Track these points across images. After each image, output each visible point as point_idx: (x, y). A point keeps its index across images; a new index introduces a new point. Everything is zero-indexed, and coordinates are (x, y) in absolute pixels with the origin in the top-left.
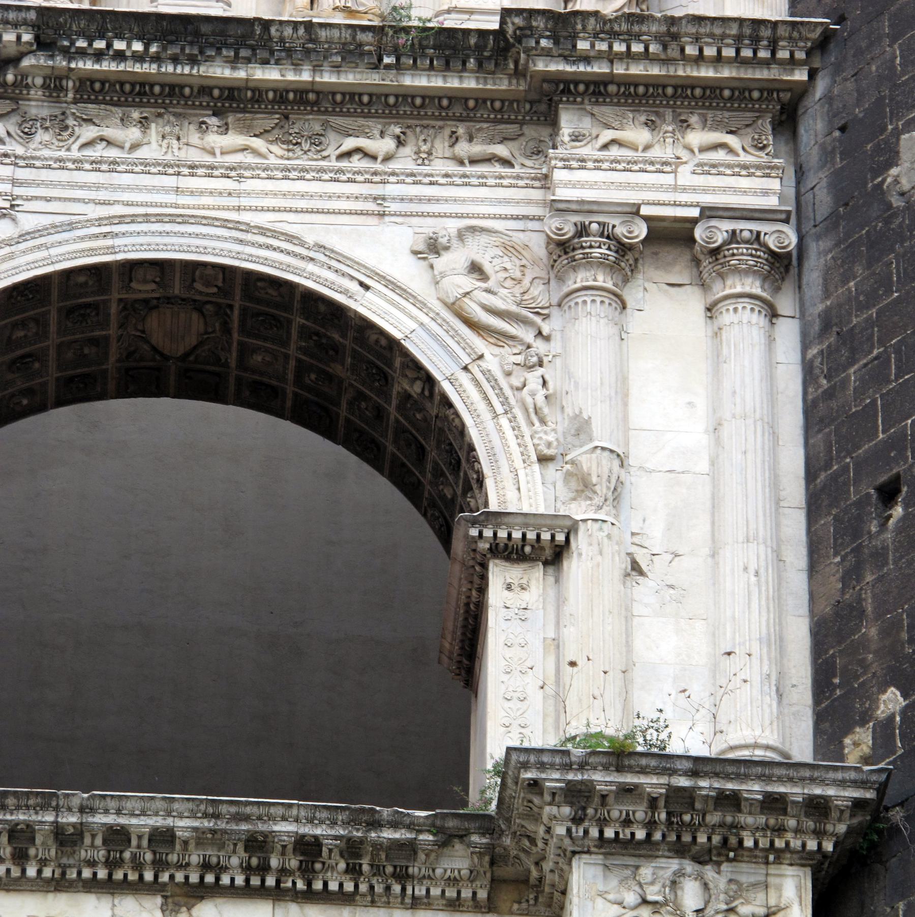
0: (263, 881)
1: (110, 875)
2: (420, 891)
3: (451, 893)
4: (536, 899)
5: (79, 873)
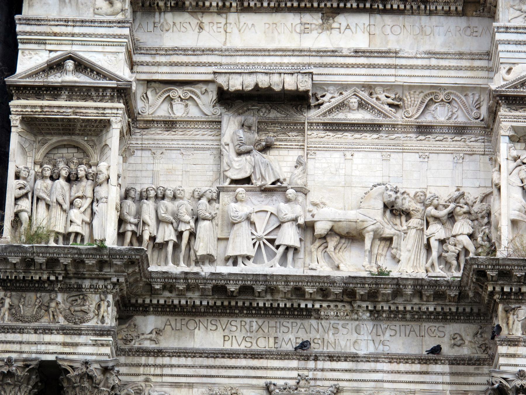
0: (365, 5)
1: (299, 5)
2: (433, 8)
3: (446, 8)
4: (483, 9)
5: (286, 4)
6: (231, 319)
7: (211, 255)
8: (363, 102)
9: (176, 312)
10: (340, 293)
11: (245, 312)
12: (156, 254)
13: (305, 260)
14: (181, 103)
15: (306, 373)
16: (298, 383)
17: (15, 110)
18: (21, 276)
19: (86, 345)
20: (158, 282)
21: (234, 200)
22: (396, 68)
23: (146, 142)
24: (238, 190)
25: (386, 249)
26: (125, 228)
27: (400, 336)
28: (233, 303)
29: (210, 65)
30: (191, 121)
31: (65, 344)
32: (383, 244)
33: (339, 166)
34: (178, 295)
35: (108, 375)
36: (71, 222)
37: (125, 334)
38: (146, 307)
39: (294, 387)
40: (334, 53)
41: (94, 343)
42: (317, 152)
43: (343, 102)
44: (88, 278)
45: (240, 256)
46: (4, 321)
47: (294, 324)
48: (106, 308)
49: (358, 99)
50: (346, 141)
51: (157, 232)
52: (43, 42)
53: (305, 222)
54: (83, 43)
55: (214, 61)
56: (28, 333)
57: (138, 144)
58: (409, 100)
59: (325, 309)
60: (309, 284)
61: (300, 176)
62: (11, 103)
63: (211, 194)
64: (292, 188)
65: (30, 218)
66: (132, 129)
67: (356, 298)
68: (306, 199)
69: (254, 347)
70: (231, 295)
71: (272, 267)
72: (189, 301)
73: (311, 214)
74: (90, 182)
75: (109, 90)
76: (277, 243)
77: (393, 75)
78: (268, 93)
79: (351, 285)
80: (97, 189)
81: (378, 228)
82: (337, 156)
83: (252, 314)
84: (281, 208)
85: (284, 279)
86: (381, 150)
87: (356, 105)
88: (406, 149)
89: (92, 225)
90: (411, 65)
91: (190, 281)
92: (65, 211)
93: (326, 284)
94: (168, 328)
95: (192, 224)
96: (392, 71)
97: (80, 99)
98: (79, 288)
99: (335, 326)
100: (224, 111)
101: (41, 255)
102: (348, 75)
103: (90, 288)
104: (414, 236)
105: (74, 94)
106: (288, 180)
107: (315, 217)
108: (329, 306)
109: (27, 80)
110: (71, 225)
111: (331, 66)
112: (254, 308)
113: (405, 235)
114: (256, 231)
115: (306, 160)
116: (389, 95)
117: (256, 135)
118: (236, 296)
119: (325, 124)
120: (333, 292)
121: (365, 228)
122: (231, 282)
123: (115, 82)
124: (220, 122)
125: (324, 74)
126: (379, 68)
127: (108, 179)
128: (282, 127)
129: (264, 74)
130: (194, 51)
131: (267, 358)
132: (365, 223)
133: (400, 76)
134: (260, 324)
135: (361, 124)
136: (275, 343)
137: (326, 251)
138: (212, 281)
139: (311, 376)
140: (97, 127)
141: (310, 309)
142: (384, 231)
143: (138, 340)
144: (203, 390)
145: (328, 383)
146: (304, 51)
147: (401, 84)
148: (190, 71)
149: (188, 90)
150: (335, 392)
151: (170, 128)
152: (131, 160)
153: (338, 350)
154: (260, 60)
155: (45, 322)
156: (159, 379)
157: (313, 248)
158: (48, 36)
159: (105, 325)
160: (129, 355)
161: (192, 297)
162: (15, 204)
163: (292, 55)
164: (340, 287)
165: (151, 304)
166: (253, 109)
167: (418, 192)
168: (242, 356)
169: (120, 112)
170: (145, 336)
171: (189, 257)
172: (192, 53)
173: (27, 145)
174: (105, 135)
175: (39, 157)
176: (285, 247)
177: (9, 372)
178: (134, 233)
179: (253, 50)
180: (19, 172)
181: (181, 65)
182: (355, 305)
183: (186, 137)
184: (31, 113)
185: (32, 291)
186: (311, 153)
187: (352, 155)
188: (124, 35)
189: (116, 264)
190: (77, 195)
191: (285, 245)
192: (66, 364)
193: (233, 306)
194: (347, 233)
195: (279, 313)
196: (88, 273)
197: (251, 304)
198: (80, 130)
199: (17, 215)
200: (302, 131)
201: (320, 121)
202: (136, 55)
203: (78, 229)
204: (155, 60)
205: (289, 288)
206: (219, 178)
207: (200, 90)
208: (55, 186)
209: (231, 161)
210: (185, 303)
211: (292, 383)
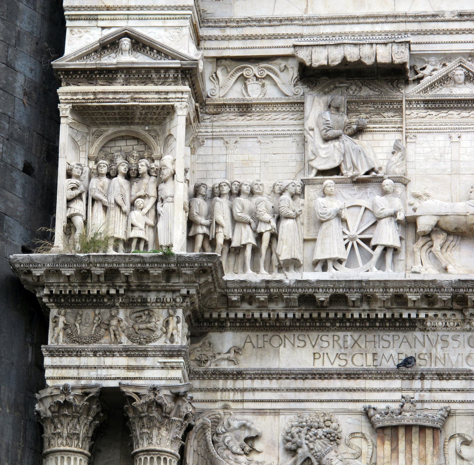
6: (321, 334)
7: (296, 259)
8: (471, 74)
9: (257, 326)
10: (449, 299)
11: (338, 325)
12: (232, 260)
13: (406, 262)
14: (257, 82)
15: (411, 394)
16: (402, 406)
17: (64, 97)
18: (77, 290)
19: (153, 368)
20: (234, 293)
21: (322, 194)
23: (217, 130)
26: (195, 230)
27: (333, 347)
28: (323, 315)
29: (289, 37)
30: (269, 104)
31: (129, 368)
33: (444, 151)
34: (259, 307)
35: (180, 403)
36: (132, 226)
37: (198, 354)
38: (222, 323)
39: (397, 412)
40: (434, 17)
41: (162, 365)
42: (418, 135)
43: (447, 75)
44: (154, 291)
45: (330, 259)
46: (58, 342)
47: (396, 338)
48: (175, 325)
49: (465, 70)
50: (452, 120)
51: (233, 234)
52: (95, 18)
53: (405, 217)
54: (141, 18)
55: (294, 32)
56: (87, 356)
57: (207, 132)
59: (432, 319)
60: (411, 290)
61: (398, 164)
62: (59, 90)
63: (294, 188)
64: (389, 178)
65: (85, 223)
66: (200, 115)
67: (468, 305)
68: (406, 190)
69: (350, 366)
70: (321, 306)
71: (368, 271)
72: (271, 313)
73: (412, 207)
74: (153, 179)
75: (172, 71)
76: (373, 243)
79: (461, 290)
80: (162, 186)
82: (441, 139)
83: (346, 327)
84: (377, 201)
85: (383, 285)
87: (462, 78)
89: (157, 229)
91: (272, 290)
92: (124, 213)
93: (432, 290)
94: (248, 345)
95: (273, 223)
97: (138, 83)
98: (144, 302)
99: (444, 338)
100: (307, 90)
101: (98, 265)
102: (452, 43)
103: (157, 302)
105: (132, 76)
106: (384, 168)
107: (417, 211)
108: (436, 316)
109: (78, 62)
110: (132, 229)
111: (432, 32)
112: (348, 320)
114: (348, 229)
115: (404, 145)
117: (346, 117)
118: (326, 307)
119: (426, 102)
120: (441, 299)
122: (321, 290)
123: (179, 61)
124: (303, 103)
125: (424, 43)
127: (173, 175)
129: (352, 46)
130: (271, 22)
131: (365, 378)
134: (356, 338)
135: (469, 100)
136: (374, 360)
137: (431, 251)
138: (298, 289)
139: (417, 398)
140: (159, 114)
141: (414, 319)
143: (213, 360)
144: (292, 417)
145: (437, 406)
146: (399, 16)
148: (267, 45)
149: (264, 68)
150: (446, 415)
151: (245, 112)
152: (201, 151)
153: (448, 366)
154: (347, 29)
155: (105, 342)
156: (239, 406)
157: (416, 247)
158: (100, 10)
159: (174, 344)
160: (204, 379)
161: (275, 308)
162: (68, 207)
163: (386, 22)
164: (448, 292)
165: (228, 319)
166: (340, 87)
168: (335, 376)
169: (186, 96)
170: (222, 356)
171: (271, 262)
172: (268, 24)
173: (79, 138)
174: (168, 123)
175: (93, 151)
176: (383, 247)
177: (65, 401)
178: (206, 236)
179: (339, 18)
180: (71, 170)
181: (256, 39)
182: (467, 314)
183: (264, 122)
184: (83, 101)
185: (90, 307)
186: (411, 136)
187: (459, 137)
188: (188, 6)
189: (185, 274)
190: (138, 194)
191: (382, 245)
192: (131, 390)
193: (323, 319)
194: (456, 229)
195: (378, 324)
196: (154, 284)
197: (344, 315)
198: (139, 119)
199: (70, 220)
200: (399, 111)
201: (420, 98)
202: (203, 29)
203: (141, 234)
204: (226, 34)
205: (389, 295)
206: (304, 169)
207: (278, 66)
208: (112, 184)
210: (267, 316)
211: (395, 406)
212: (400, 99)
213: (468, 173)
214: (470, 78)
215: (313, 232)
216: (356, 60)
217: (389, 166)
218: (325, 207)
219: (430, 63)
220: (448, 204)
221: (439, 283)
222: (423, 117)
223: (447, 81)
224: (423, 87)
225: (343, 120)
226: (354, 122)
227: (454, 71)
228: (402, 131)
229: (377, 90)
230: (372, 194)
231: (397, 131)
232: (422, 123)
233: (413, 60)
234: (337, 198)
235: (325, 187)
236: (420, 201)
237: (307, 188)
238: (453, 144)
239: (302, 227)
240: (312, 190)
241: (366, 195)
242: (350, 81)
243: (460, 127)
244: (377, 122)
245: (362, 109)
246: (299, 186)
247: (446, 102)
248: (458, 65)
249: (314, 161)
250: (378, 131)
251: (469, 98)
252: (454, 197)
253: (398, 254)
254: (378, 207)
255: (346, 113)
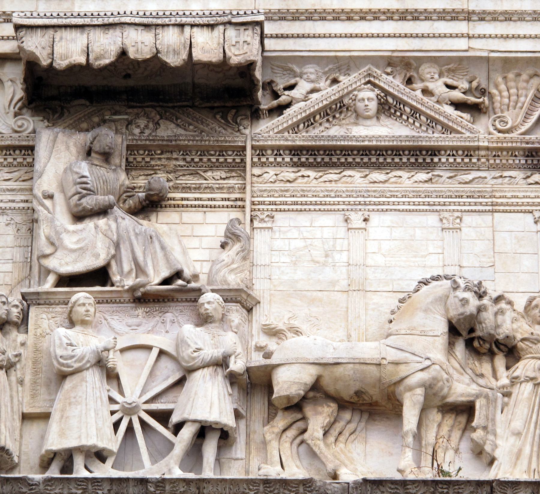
8: (390, 100)
22: (469, 20)
24: (74, 298)
25: (456, 434)
32: (449, 420)
33: (334, 246)
42: (278, 216)
43: (340, 100)
45: (80, 449)
49: (377, 91)
50: (350, 187)
58: (505, 94)
61: (234, 266)
63: (5, 307)
64: (213, 291)
68: (250, 321)
76: (175, 419)
77: (463, 36)
78: (154, 83)
81: (435, 379)
86: (438, 208)
87: (373, 106)
88: (502, 204)
90: (505, 13)
96: (462, 27)
102: (351, 36)
104: (529, 399)
107: (274, 357)
113: (506, 399)
114: (121, 392)
115: (249, 232)
116: (455, 83)
117: (123, 176)
119: (295, 151)
121: (402, 380)
124: (32, 149)
125: (293, 37)
126: (426, 19)
128: (189, 159)
129: (140, 28)
132: (402, 367)
133: (479, 37)
135: (386, 149)
137: (302, 442)
142: (450, 388)
147: (485, 54)
166: (114, 121)
167: (534, 298)
186: (261, 217)
187: (365, 220)
191: (195, 421)
194: (358, 393)
201: (282, 143)
206: (29, 277)
209: (58, 233)
212: (240, 144)
213: (385, 289)
214: (390, 108)
215: (45, 400)
216: (148, 57)
217: (214, 271)
218: (71, 345)
219: (305, 76)
220: (342, 346)
221: (320, 487)
222: (289, 181)
223: (341, 113)
224: (290, 122)
225: (118, 180)
226: (140, 187)
227: (355, 93)
228: (244, 207)
229: (191, 127)
230: (176, 324)
231: (232, 207)
232: (287, 191)
233: (269, 71)
234: (99, 331)
235: (72, 307)
236: (279, 341)
237: (33, 312)
238: (351, 233)
239: (20, 389)
240: (44, 316)
241: (162, 325)
242: (136, 110)
243: (367, 200)
244: (189, 188)
245: (159, 163)
246: (17, 306)
247: (338, 152)
248: (363, 81)
249: (51, 258)
250: (191, 206)
251: (387, 143)
252: (353, 336)
253: (231, 446)
254: (189, 346)
255: (124, 167)
